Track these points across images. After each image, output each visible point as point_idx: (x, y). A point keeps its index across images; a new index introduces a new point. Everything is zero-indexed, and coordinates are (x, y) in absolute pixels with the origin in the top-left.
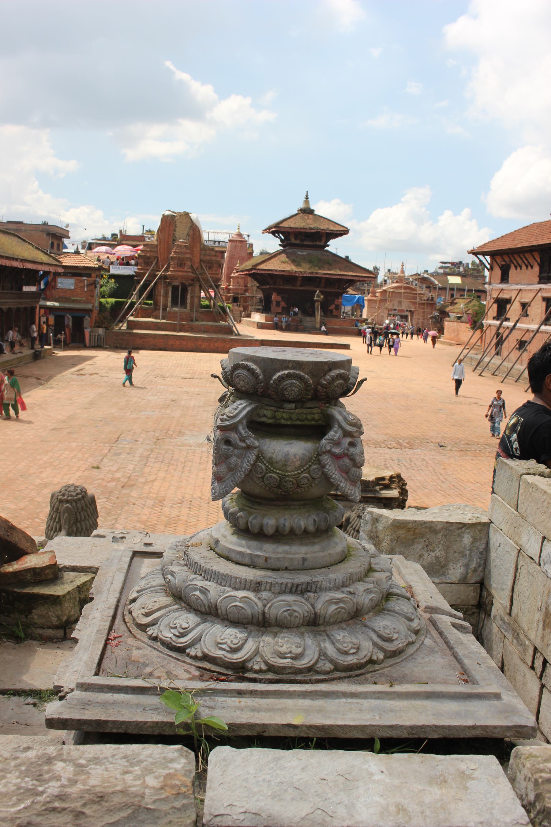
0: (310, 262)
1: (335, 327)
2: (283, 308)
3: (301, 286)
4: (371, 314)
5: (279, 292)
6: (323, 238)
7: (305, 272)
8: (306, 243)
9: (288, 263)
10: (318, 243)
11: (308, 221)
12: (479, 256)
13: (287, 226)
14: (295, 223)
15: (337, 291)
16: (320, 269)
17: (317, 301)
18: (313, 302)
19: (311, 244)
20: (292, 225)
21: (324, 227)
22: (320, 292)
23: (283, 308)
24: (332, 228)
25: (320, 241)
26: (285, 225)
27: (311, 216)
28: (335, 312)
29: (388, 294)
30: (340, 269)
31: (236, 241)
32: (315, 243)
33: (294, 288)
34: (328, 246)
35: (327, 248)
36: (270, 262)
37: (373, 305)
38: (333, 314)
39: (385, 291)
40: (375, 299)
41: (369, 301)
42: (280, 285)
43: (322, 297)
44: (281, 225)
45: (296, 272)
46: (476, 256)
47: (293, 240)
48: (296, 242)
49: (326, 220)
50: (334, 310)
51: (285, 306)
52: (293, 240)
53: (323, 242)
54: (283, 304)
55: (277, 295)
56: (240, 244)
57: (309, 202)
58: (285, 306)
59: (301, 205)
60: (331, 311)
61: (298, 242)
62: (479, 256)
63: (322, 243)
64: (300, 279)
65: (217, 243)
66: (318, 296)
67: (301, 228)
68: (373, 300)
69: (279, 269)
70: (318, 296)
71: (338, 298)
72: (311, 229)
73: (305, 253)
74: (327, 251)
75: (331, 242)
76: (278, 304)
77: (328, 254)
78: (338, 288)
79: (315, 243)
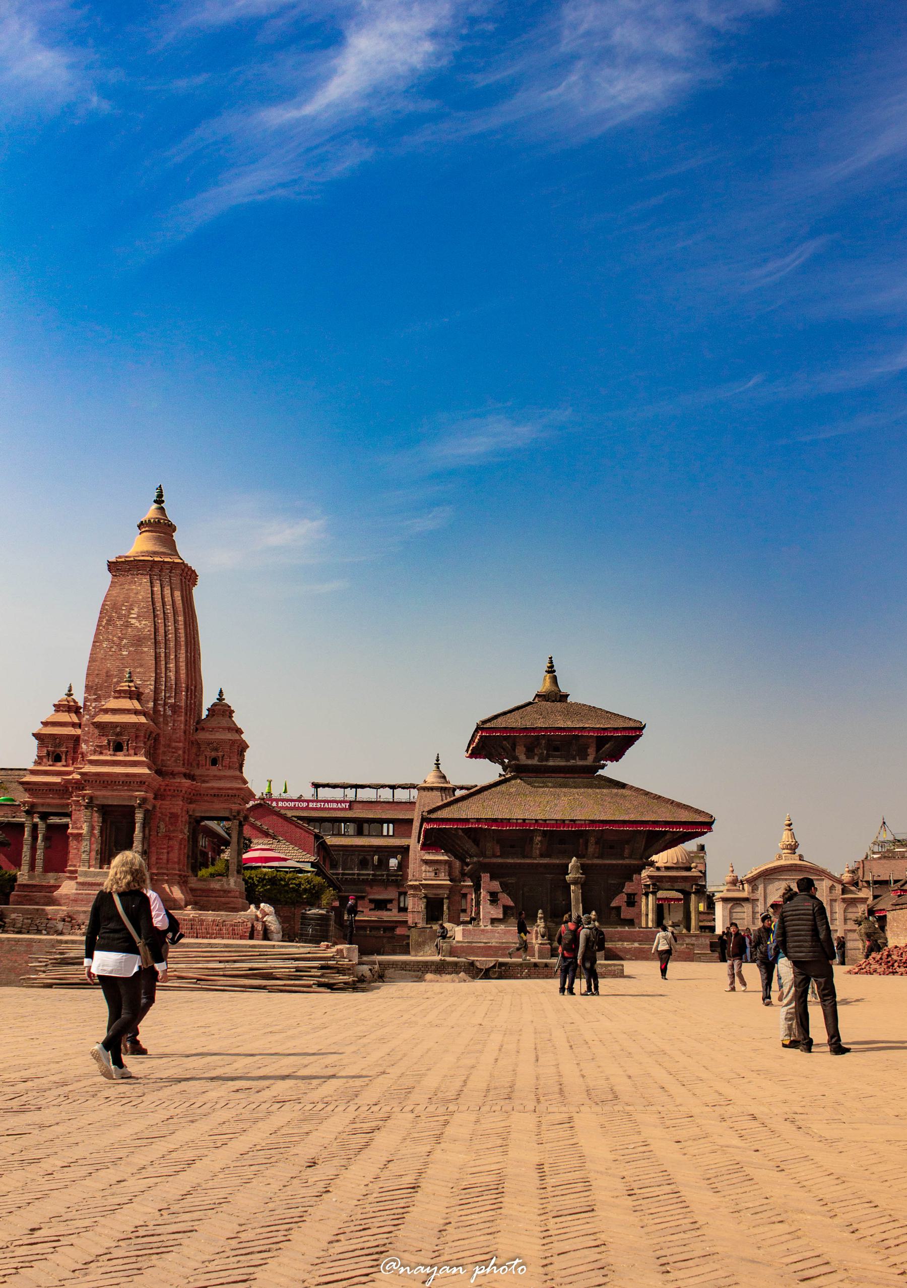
2: (506, 909)
3: (542, 856)
8: (551, 763)
15: (627, 861)
19: (563, 764)
26: (500, 723)
34: (603, 767)
42: (495, 856)
48: (530, 762)
50: (624, 908)
52: (523, 760)
53: (591, 758)
55: (492, 878)
61: (535, 762)
63: (589, 761)
78: (630, 857)
79: (572, 762)
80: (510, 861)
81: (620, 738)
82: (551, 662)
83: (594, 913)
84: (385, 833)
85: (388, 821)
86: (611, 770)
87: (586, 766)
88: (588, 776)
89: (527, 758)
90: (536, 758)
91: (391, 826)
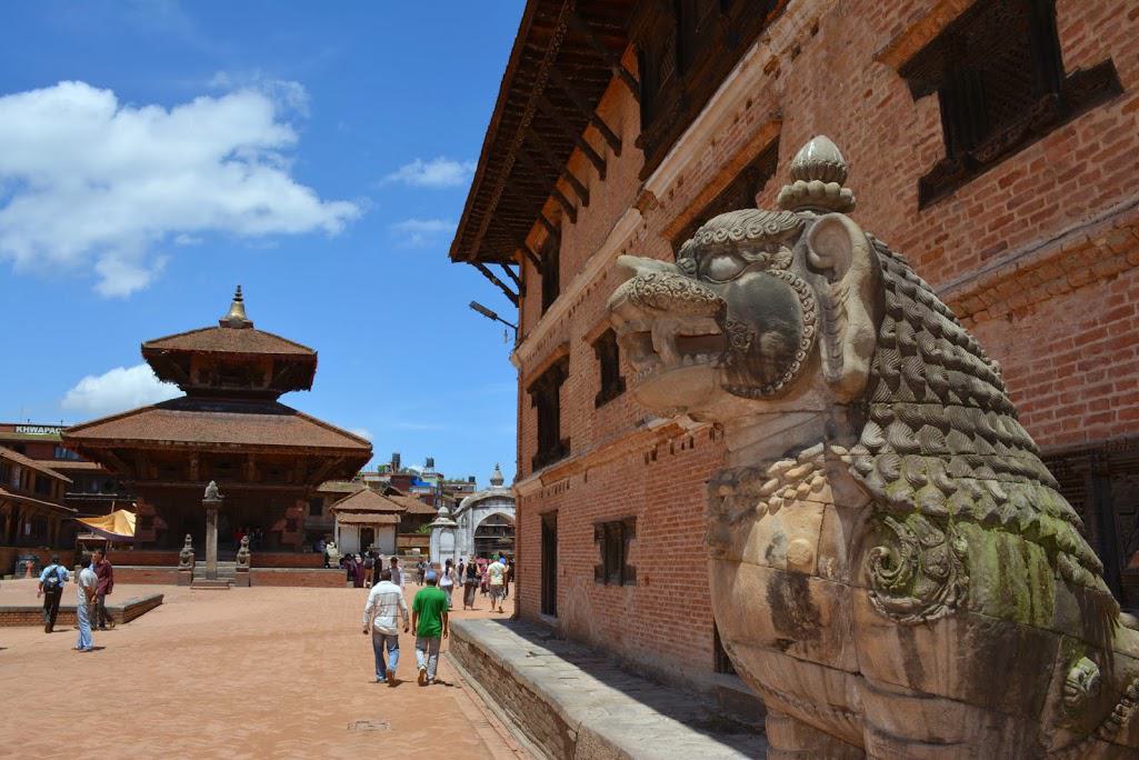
2: (159, 532)
6: (265, 377)
10: (254, 388)
12: (488, 266)
19: (237, 389)
23: (159, 532)
38: (284, 540)
48: (201, 386)
50: (284, 532)
51: (165, 526)
53: (266, 384)
58: (165, 526)
61: (208, 386)
62: (488, 266)
80: (166, 484)
81: (300, 370)
83: (188, 536)
84: (57, 456)
86: (287, 399)
88: (265, 403)
90: (210, 382)
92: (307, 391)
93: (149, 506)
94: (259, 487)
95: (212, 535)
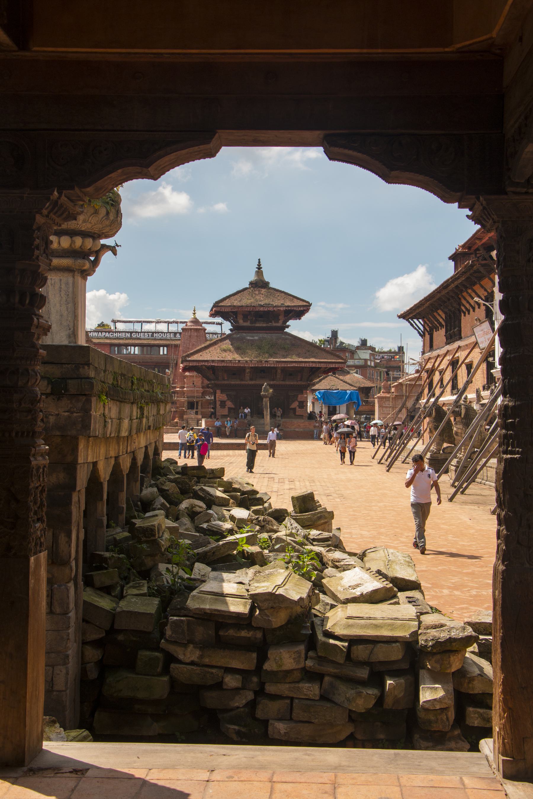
0: (260, 348)
1: (297, 430)
2: (230, 409)
3: (251, 379)
4: (384, 416)
5: (224, 389)
6: (280, 317)
7: (251, 361)
8: (258, 325)
9: (230, 351)
10: (274, 324)
11: (258, 297)
13: (229, 304)
14: (240, 301)
15: (299, 383)
16: (271, 356)
17: (266, 396)
18: (261, 398)
19: (265, 325)
20: (236, 303)
21: (277, 302)
22: (268, 384)
23: (230, 409)
24: (288, 303)
25: (277, 321)
26: (227, 303)
27: (263, 291)
28: (299, 411)
29: (404, 388)
30: (299, 355)
31: (191, 329)
32: (270, 324)
33: (243, 383)
34: (288, 327)
35: (287, 330)
36: (207, 351)
37: (387, 404)
38: (297, 414)
39: (401, 384)
40: (388, 395)
41: (379, 398)
42: (224, 380)
43: (271, 390)
44: (221, 304)
45: (239, 361)
46: (408, 320)
47: (241, 322)
48: (245, 324)
49: (283, 294)
50: (297, 409)
51: (233, 406)
52: (241, 322)
53: (281, 322)
54: (229, 404)
56: (196, 334)
57: (262, 272)
58: (233, 406)
59: (252, 277)
60: (294, 409)
61: (248, 324)
63: (280, 324)
64: (248, 370)
65: (178, 335)
66: (267, 390)
67: (247, 306)
68: (386, 397)
69: (217, 359)
70: (266, 390)
71: (302, 393)
72: (261, 306)
73: (256, 338)
74: (286, 332)
75: (290, 322)
76: (223, 404)
77: (287, 336)
78: (301, 380)
79: (270, 324)
81: (300, 310)
82: (259, 262)
85: (164, 346)
87: (278, 327)
89: (244, 322)
91: (165, 348)
92: (298, 320)
93: (224, 395)
94: (283, 383)
95: (267, 412)
